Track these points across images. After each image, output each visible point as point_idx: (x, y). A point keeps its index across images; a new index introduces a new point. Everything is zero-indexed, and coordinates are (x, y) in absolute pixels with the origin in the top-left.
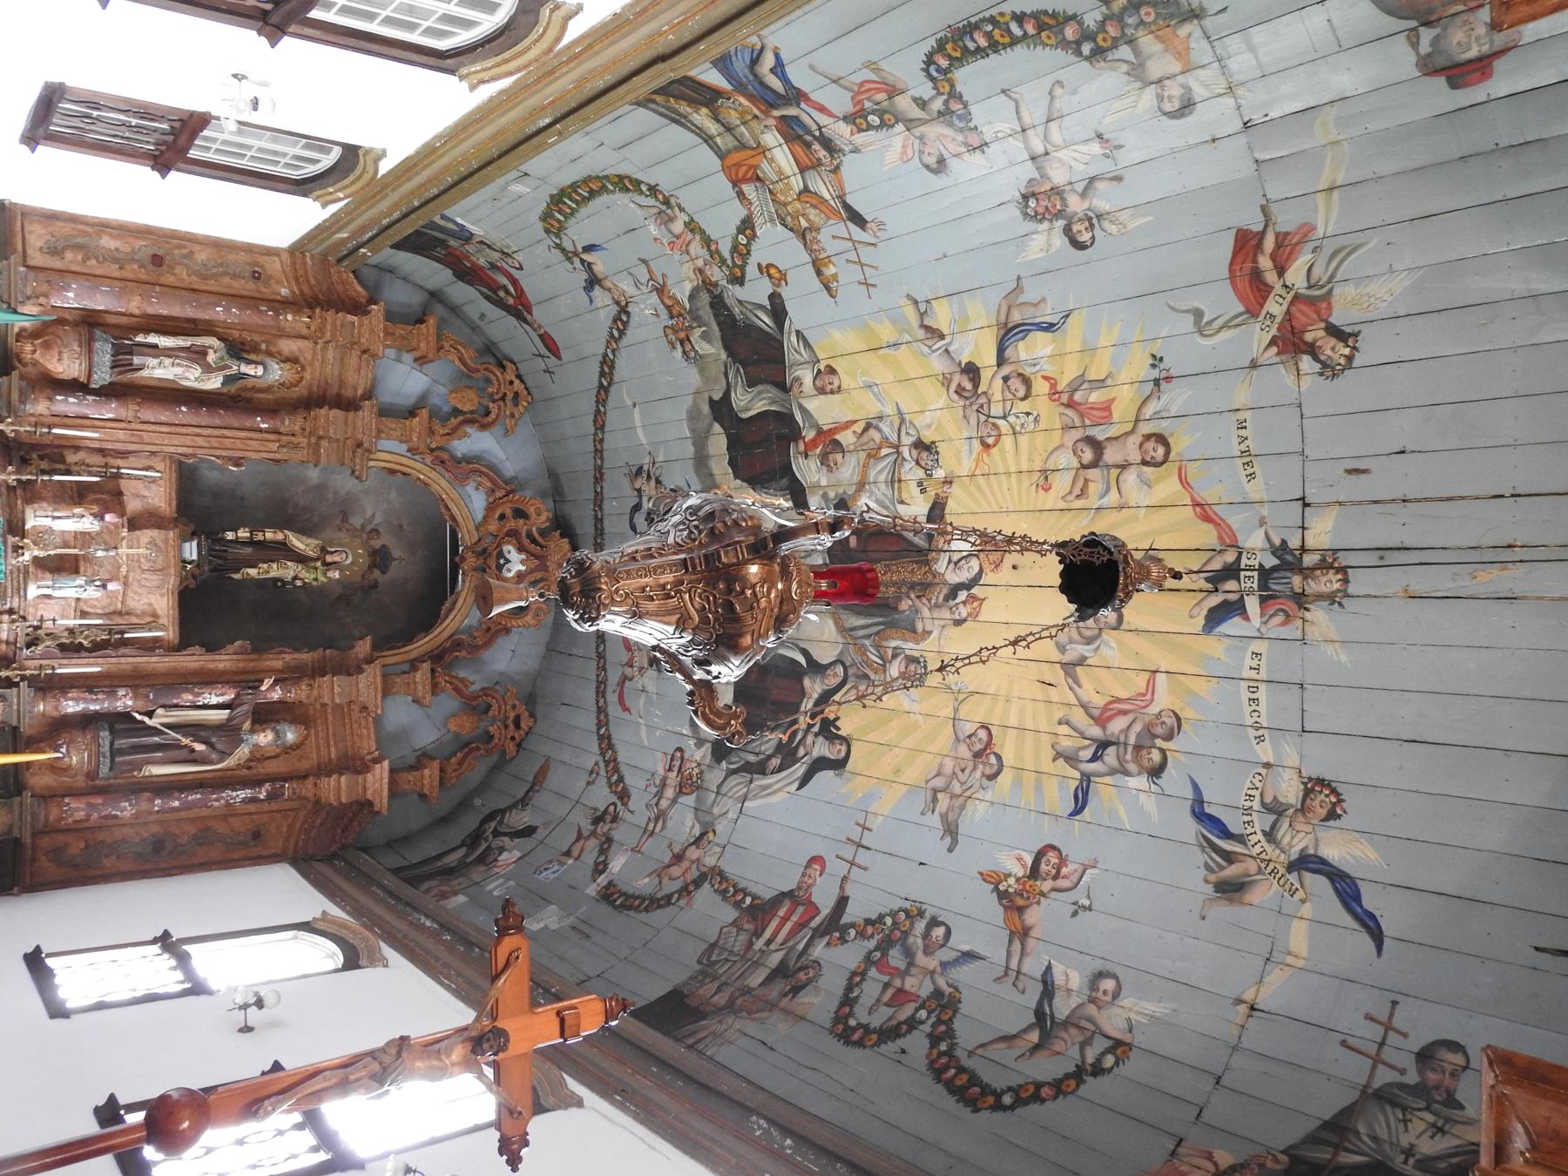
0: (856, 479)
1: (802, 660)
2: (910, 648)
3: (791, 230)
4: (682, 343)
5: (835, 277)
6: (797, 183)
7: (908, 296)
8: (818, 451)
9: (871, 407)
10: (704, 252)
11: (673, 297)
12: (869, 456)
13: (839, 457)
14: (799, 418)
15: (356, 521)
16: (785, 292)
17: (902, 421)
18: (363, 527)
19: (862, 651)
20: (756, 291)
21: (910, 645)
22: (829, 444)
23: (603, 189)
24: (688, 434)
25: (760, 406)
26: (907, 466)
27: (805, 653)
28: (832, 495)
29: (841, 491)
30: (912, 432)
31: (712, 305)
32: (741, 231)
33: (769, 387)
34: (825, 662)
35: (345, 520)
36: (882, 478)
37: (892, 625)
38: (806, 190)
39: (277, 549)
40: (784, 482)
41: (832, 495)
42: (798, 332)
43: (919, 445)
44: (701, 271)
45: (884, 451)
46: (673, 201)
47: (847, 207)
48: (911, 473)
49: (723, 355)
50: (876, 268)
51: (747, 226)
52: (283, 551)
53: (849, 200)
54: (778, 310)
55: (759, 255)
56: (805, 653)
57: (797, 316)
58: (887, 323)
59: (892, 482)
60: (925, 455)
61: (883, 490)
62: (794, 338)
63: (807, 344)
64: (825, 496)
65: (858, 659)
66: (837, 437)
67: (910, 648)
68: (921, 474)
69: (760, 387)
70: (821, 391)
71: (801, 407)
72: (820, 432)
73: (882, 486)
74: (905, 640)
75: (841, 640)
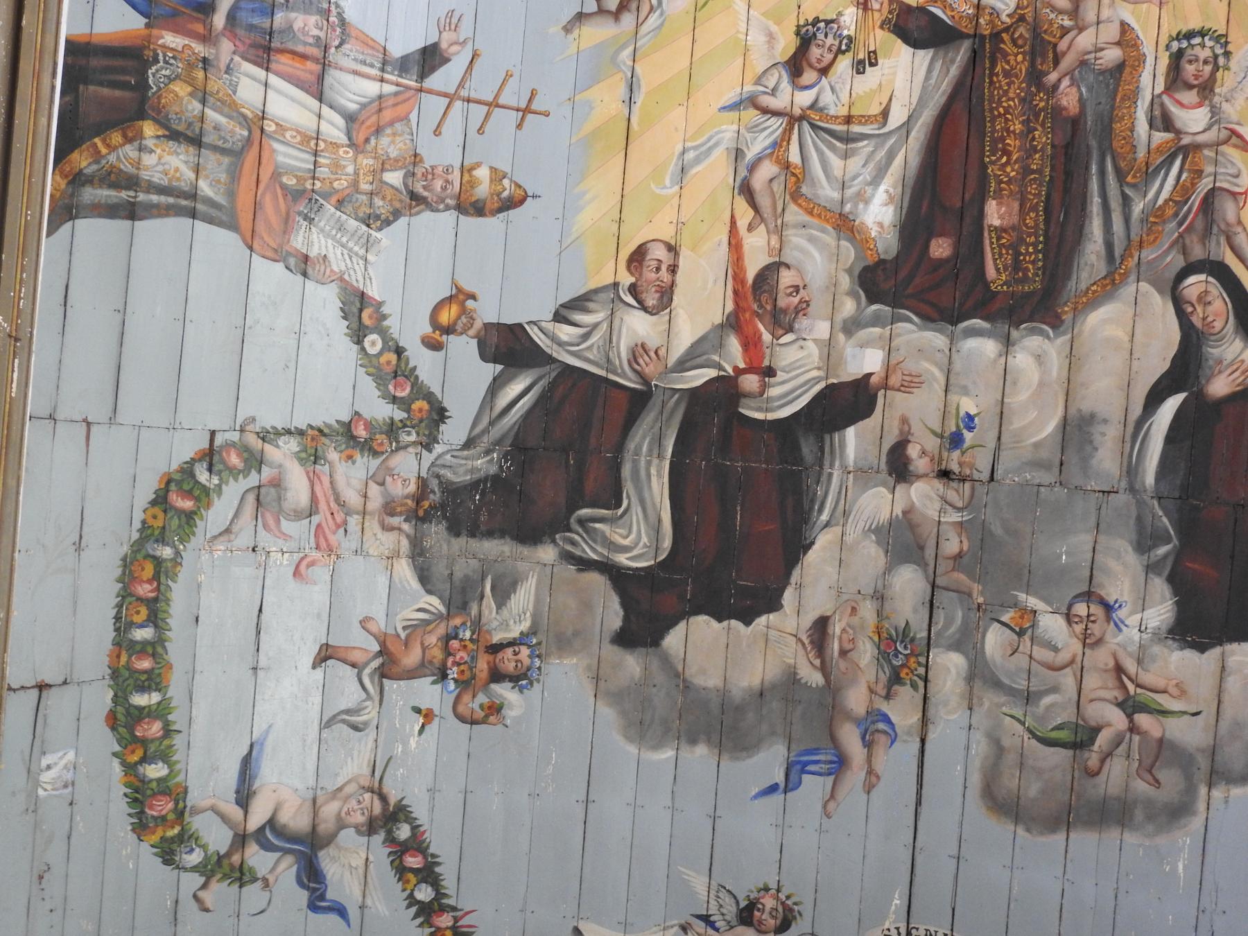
0: (829, 238)
1: (1171, 406)
2: (1151, 80)
3: (397, 214)
4: (497, 676)
5: (497, 176)
6: (334, 128)
7: (567, 29)
8: (767, 337)
9: (716, 174)
10: (363, 466)
11: (415, 628)
12: (796, 196)
13: (786, 278)
14: (699, 377)
16: (488, 311)
17: (752, 101)
19: (1156, 215)
20: (462, 378)
21: (1146, 78)
22: (761, 302)
23: (162, 572)
24: (669, 753)
25: (659, 488)
26: (827, 99)
27: (1155, 398)
28: (848, 307)
29: (845, 282)
30: (771, 84)
31: (455, 530)
32: (358, 335)
33: (631, 445)
34: (1176, 335)
36: (835, 162)
37: (1109, 124)
38: (350, 118)
40: (807, 449)
41: (848, 307)
42: (559, 317)
43: (795, 65)
44: (389, 508)
45: (794, 157)
46: (253, 441)
47: (403, 65)
48: (841, 90)
49: (547, 553)
50: (509, 75)
51: (360, 313)
53: (397, 50)
54: (509, 347)
55: (409, 326)
56: (1155, 398)
57: (529, 305)
58: (594, 94)
59: (848, 139)
60: (815, 52)
61: (857, 165)
62: (566, 332)
63: (580, 303)
64: (851, 327)
65: (1171, 230)
66: (750, 275)
67: (1151, 80)
68: (844, 65)
69: (626, 471)
70: (667, 294)
71: (684, 364)
72: (735, 323)
73: (855, 163)
74: (1133, 96)
75: (1129, 290)
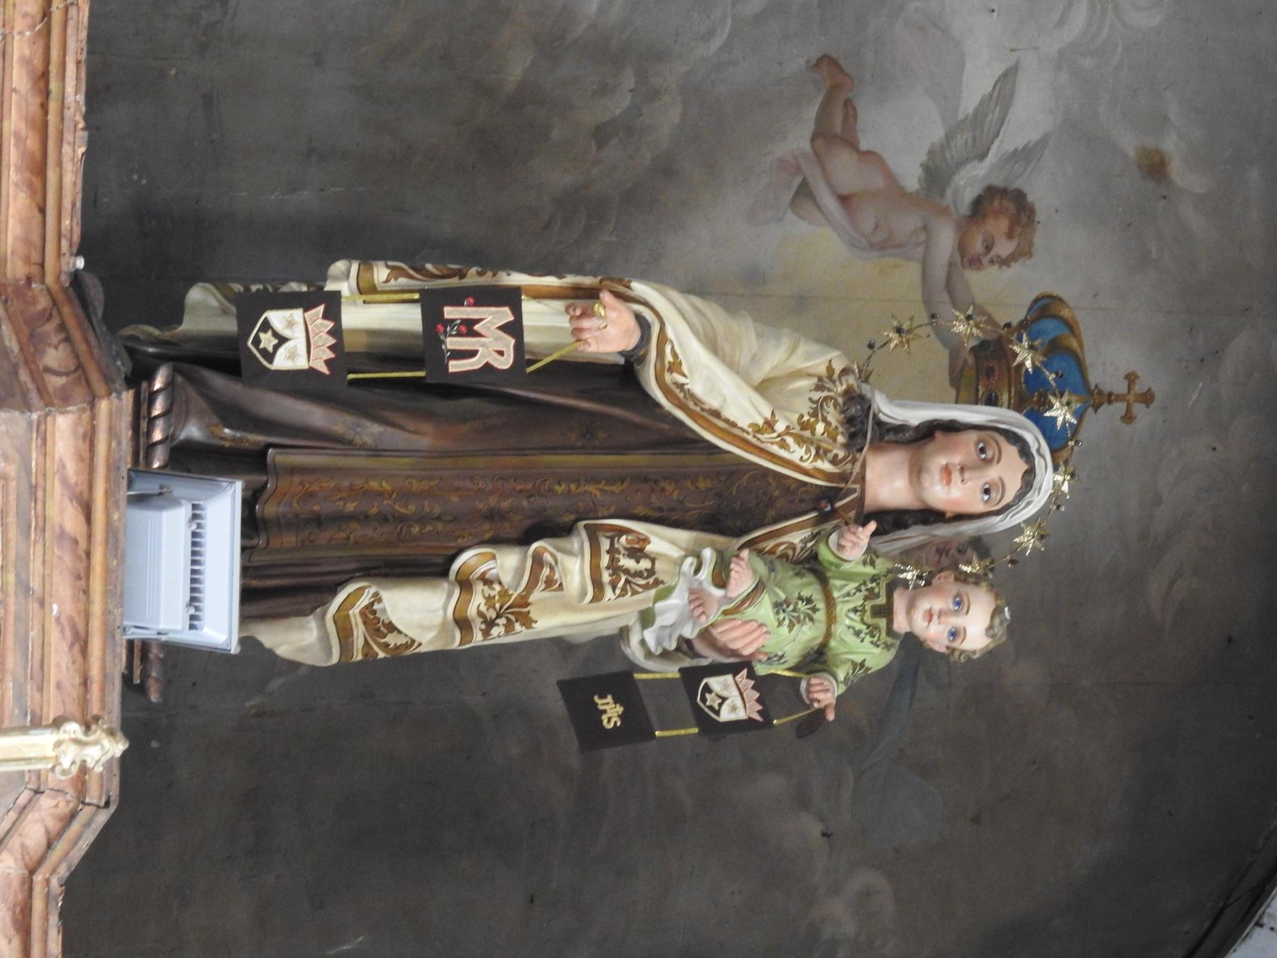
15: (902, 134)
18: (937, 175)
35: (836, 130)
39: (590, 432)
52: (599, 442)
